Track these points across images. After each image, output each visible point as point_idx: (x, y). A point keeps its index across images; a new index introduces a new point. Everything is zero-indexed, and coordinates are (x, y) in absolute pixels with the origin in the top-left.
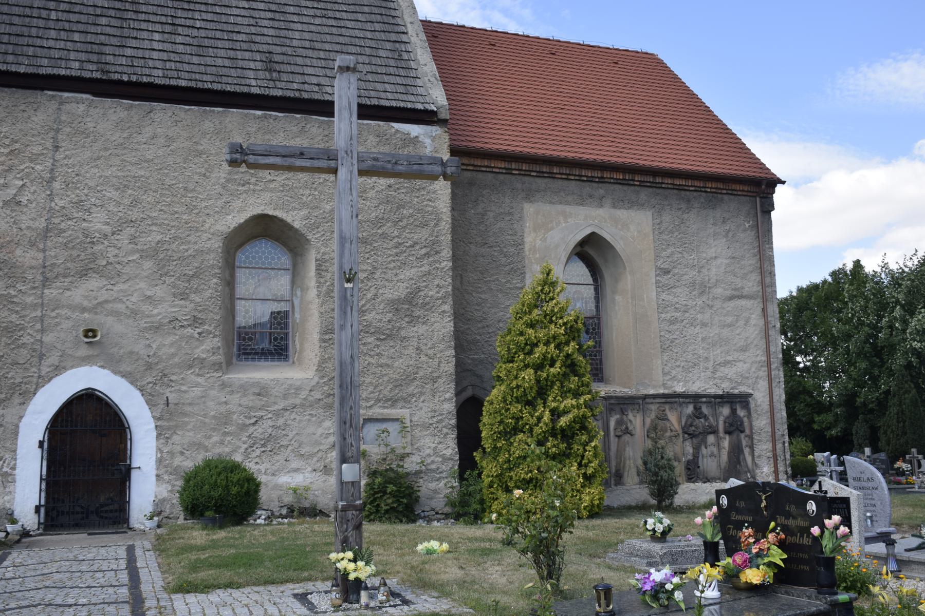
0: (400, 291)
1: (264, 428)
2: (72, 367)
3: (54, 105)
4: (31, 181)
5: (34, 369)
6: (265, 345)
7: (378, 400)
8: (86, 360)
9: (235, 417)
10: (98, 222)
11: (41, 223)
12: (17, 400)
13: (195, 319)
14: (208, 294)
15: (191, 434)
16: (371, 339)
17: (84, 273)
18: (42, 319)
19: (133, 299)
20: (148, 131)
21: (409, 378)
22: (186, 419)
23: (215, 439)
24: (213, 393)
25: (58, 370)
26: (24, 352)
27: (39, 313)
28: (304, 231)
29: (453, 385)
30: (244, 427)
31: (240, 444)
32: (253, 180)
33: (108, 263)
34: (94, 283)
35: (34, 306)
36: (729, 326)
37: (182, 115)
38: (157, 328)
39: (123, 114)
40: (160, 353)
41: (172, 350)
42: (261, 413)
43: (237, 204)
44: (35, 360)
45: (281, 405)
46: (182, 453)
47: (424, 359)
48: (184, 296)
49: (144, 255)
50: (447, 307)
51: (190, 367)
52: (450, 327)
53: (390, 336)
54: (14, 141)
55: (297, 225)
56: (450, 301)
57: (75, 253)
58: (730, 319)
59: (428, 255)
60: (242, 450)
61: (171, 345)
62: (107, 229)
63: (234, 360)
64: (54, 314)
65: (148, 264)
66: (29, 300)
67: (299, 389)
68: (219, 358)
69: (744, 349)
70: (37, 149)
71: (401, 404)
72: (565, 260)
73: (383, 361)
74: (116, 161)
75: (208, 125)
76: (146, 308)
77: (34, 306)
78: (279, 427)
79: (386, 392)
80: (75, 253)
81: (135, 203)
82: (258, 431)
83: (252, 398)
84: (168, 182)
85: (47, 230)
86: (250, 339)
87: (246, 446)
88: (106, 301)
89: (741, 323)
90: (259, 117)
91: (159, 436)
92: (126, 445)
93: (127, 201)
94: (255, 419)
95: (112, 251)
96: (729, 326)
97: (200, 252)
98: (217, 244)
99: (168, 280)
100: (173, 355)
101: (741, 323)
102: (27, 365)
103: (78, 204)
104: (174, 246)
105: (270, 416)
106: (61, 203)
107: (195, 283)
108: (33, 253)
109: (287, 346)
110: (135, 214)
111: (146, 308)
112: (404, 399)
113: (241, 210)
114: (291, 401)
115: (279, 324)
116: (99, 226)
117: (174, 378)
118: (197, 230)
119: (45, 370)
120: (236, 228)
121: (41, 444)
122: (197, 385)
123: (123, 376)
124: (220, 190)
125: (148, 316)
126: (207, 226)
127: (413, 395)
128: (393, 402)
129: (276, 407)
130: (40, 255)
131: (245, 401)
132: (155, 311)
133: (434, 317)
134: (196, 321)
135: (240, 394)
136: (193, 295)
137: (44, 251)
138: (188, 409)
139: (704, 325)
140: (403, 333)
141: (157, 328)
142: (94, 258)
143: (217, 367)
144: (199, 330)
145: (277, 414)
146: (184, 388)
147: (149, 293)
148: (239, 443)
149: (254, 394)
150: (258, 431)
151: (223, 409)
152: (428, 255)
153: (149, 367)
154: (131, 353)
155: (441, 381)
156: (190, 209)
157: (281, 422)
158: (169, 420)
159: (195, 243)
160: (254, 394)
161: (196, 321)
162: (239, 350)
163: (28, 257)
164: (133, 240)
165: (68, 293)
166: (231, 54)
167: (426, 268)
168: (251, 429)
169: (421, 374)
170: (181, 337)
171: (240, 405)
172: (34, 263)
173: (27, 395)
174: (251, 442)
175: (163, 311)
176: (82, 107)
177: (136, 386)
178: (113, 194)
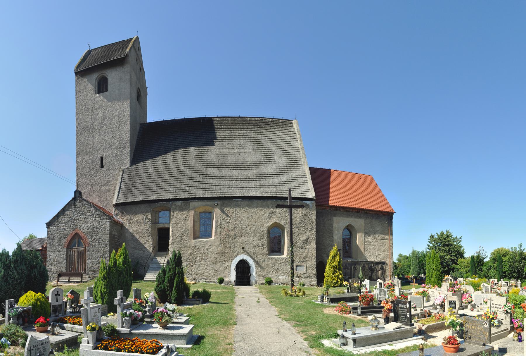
0: (305, 238)
6: (276, 250)
7: (299, 262)
8: (242, 253)
11: (233, 227)
12: (230, 261)
14: (265, 240)
16: (298, 249)
17: (241, 236)
19: (251, 241)
21: (306, 257)
27: (234, 244)
29: (315, 259)
30: (272, 267)
36: (381, 246)
42: (275, 264)
45: (280, 262)
47: (309, 253)
50: (315, 242)
52: (315, 246)
53: (302, 248)
54: (228, 210)
55: (282, 225)
56: (315, 240)
58: (381, 245)
59: (310, 230)
62: (246, 227)
67: (283, 259)
68: (267, 253)
69: (384, 251)
70: (232, 212)
71: (304, 262)
72: (343, 230)
73: (301, 253)
74: (247, 213)
76: (253, 242)
79: (301, 260)
80: (240, 232)
81: (250, 221)
84: (257, 216)
85: (235, 228)
89: (384, 245)
93: (249, 221)
96: (381, 246)
98: (266, 229)
100: (259, 252)
101: (384, 245)
106: (237, 222)
107: (262, 237)
109: (281, 250)
110: (250, 224)
112: (305, 262)
113: (271, 222)
114: (281, 262)
116: (244, 226)
127: (307, 261)
128: (303, 262)
130: (234, 233)
131: (272, 261)
133: (312, 244)
139: (375, 246)
140: (305, 247)
142: (243, 233)
143: (267, 254)
145: (279, 264)
151: (268, 263)
152: (310, 230)
155: (313, 258)
157: (279, 266)
161: (262, 245)
163: (232, 233)
164: (250, 229)
165: (239, 240)
167: (310, 233)
168: (274, 267)
169: (309, 256)
178: (246, 220)
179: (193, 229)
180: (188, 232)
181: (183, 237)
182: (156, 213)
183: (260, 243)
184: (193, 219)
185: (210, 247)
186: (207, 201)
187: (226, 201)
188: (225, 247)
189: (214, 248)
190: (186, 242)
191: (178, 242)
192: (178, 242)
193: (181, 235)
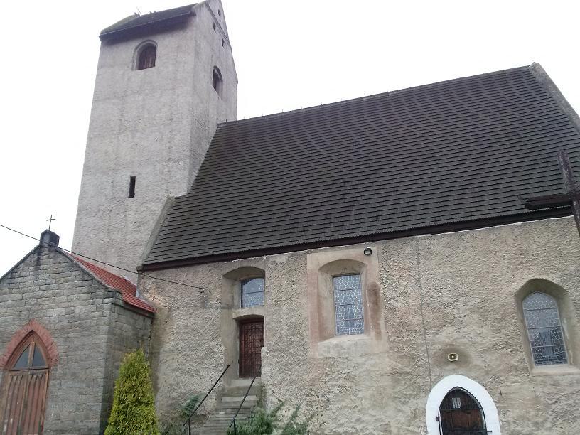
1: (561, 406)
2: (447, 375)
3: (414, 243)
4: (410, 281)
5: (428, 378)
6: (552, 355)
9: (542, 399)
10: (446, 297)
11: (419, 301)
13: (507, 344)
15: (518, 411)
17: (443, 325)
18: (427, 351)
20: (462, 246)
22: (514, 402)
23: (532, 413)
24: (526, 386)
25: (440, 377)
26: (421, 369)
28: (561, 284)
30: (548, 406)
31: (549, 416)
32: (524, 261)
33: (455, 318)
34: (450, 329)
35: (422, 345)
37: (478, 234)
38: (487, 351)
39: (448, 240)
40: (491, 364)
41: (498, 362)
43: (518, 275)
44: (427, 373)
45: (569, 391)
46: (515, 423)
48: (498, 331)
49: (473, 311)
51: (510, 371)
55: (555, 282)
57: (437, 314)
60: (550, 420)
61: (497, 359)
63: (534, 364)
64: (432, 348)
65: (475, 316)
66: (419, 341)
75: (492, 236)
76: (479, 340)
77: (422, 345)
78: (571, 405)
82: (558, 407)
83: (550, 387)
86: (541, 352)
87: (552, 417)
88: (457, 338)
90: (520, 226)
91: (499, 413)
92: (481, 417)
93: (458, 284)
94: (554, 401)
95: (456, 311)
97: (502, 305)
98: (511, 300)
99: (489, 323)
100: (499, 366)
102: (424, 376)
103: (435, 289)
104: (487, 304)
105: (563, 398)
107: (503, 323)
108: (417, 317)
110: (463, 290)
111: (479, 340)
113: (521, 278)
115: (557, 341)
117: (501, 378)
118: (498, 293)
119: (433, 378)
120: (520, 289)
121: (438, 418)
122: (516, 382)
123: (474, 379)
124: (507, 270)
125: (481, 344)
126: (503, 290)
129: (566, 392)
130: (421, 318)
131: (546, 390)
132: (485, 341)
134: (508, 345)
135: (542, 386)
136: (503, 330)
137: (422, 315)
138: (513, 396)
141: (487, 351)
143: (526, 370)
144: (511, 350)
145: (568, 396)
146: (508, 384)
147: (478, 332)
148: (549, 416)
149: (551, 385)
150: (558, 407)
153: (487, 373)
154: (476, 365)
156: (492, 283)
158: (503, 403)
159: (499, 301)
160: (551, 385)
161: (508, 345)
162: (535, 359)
163: (414, 320)
164: (465, 304)
166: (497, 196)
168: (554, 406)
170: (502, 354)
171: (544, 392)
172: (419, 322)
173: (427, 392)
174: (554, 415)
175: (489, 340)
176: (428, 241)
177: (481, 384)
179: (316, 314)
180: (306, 322)
181: (294, 338)
182: (233, 285)
183: (500, 339)
184: (316, 291)
185: (363, 359)
186: (348, 248)
187: (393, 244)
188: (404, 355)
189: (373, 362)
190: (302, 349)
191: (282, 350)
192: (282, 350)
193: (289, 332)
